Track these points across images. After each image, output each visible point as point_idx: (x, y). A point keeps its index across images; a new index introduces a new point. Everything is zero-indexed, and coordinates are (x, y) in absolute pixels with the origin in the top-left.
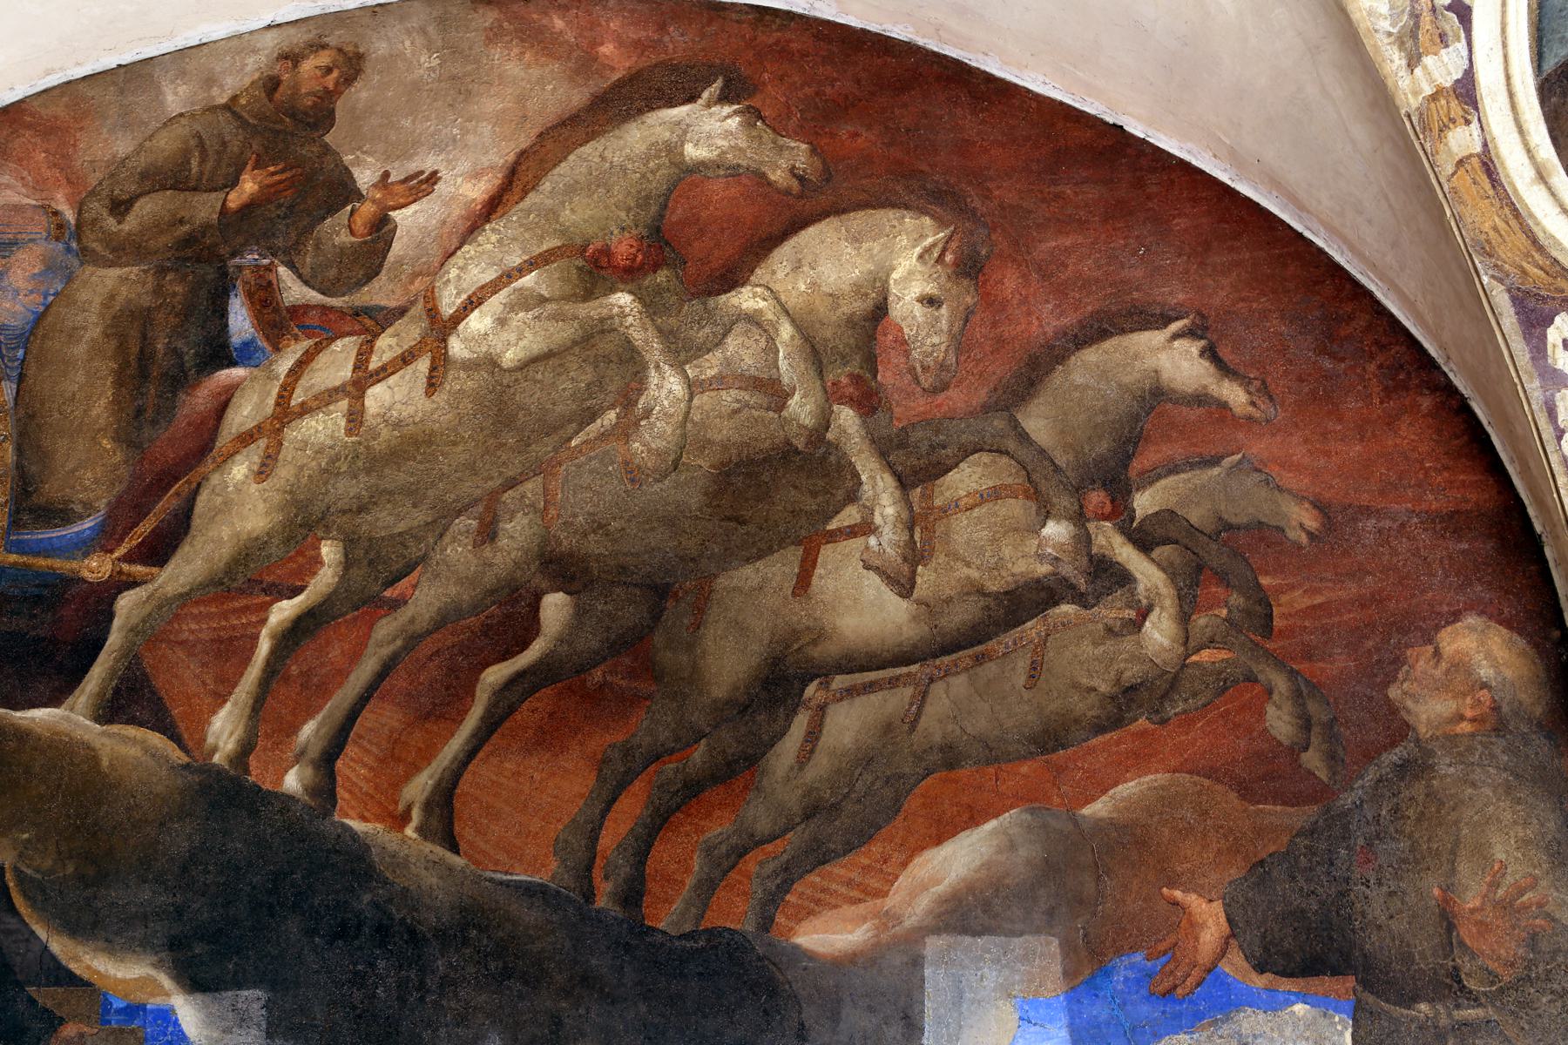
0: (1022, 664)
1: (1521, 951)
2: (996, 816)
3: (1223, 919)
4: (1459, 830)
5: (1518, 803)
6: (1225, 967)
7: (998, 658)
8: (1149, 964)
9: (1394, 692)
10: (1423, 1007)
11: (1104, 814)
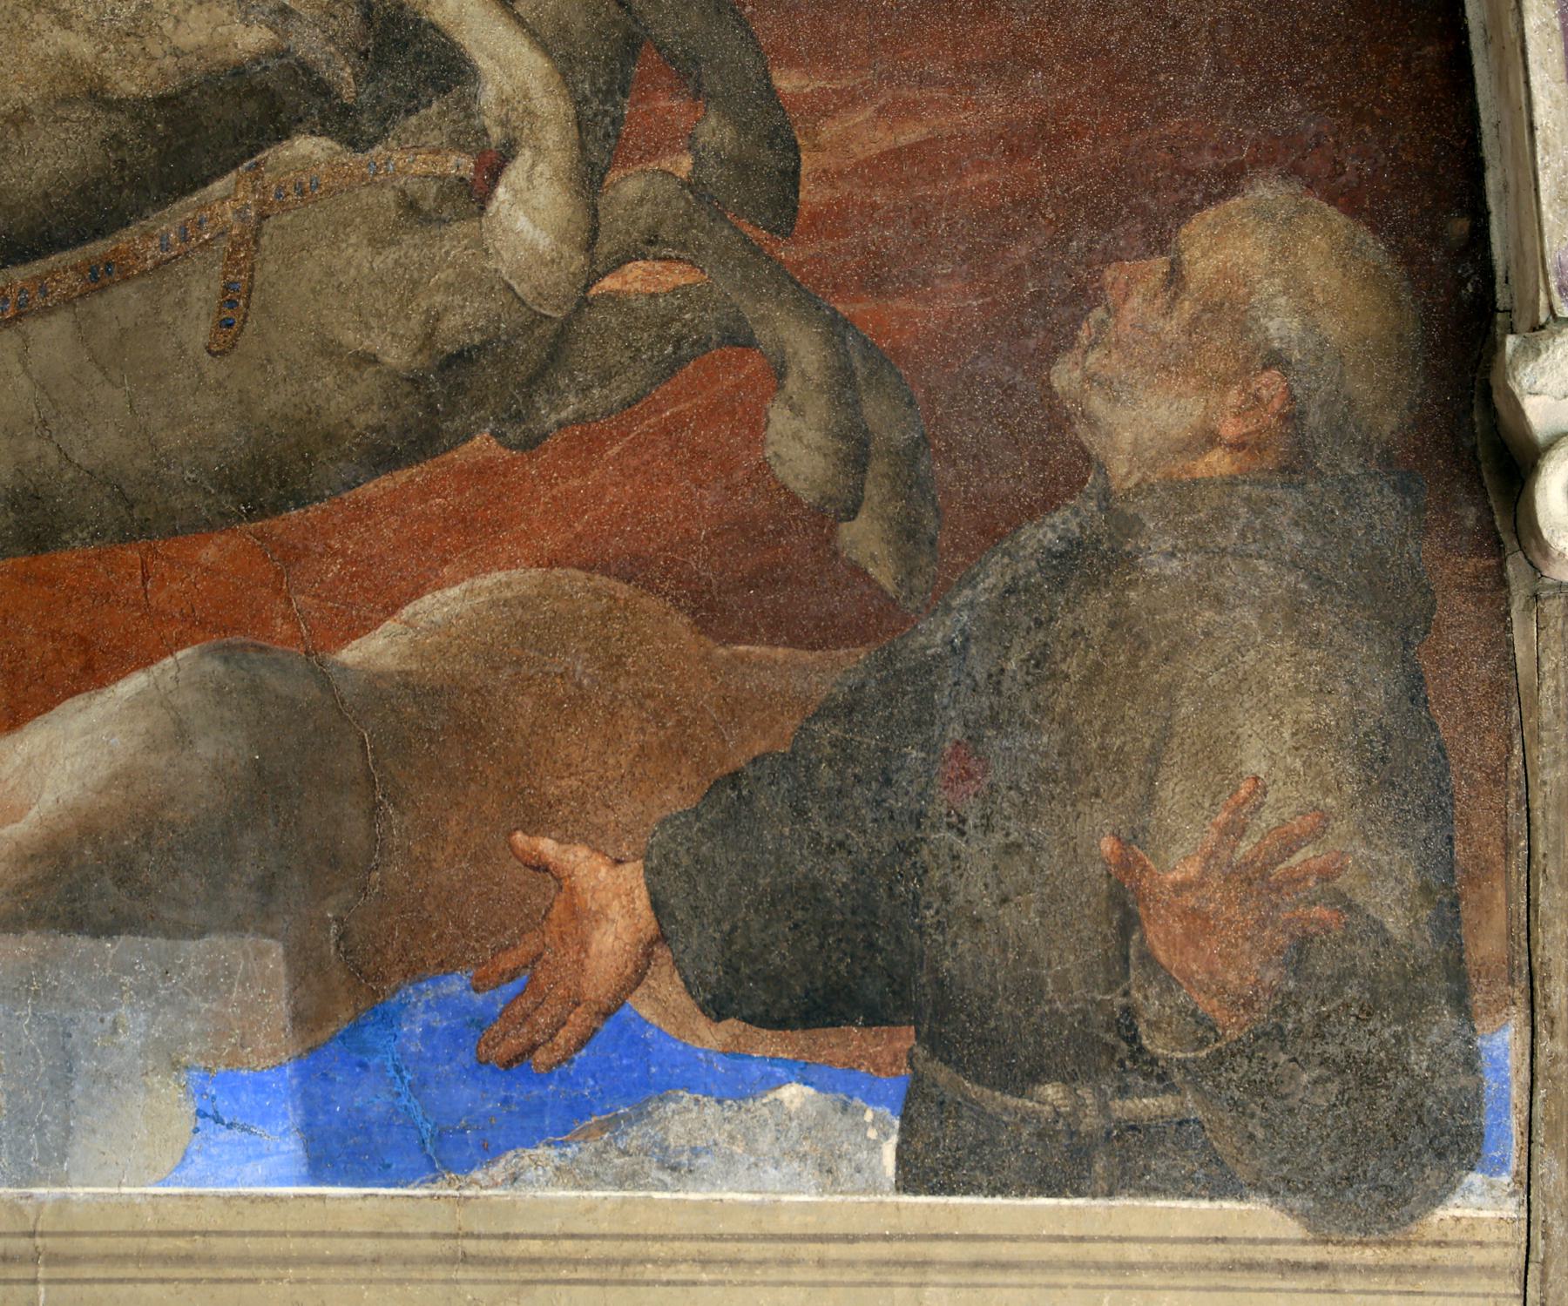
0: (203, 290)
1: (1271, 975)
2: (144, 662)
3: (642, 903)
4: (1173, 705)
5: (1312, 645)
6: (641, 1006)
7: (143, 273)
8: (479, 999)
9: (1064, 376)
10: (1051, 1091)
11: (389, 662)
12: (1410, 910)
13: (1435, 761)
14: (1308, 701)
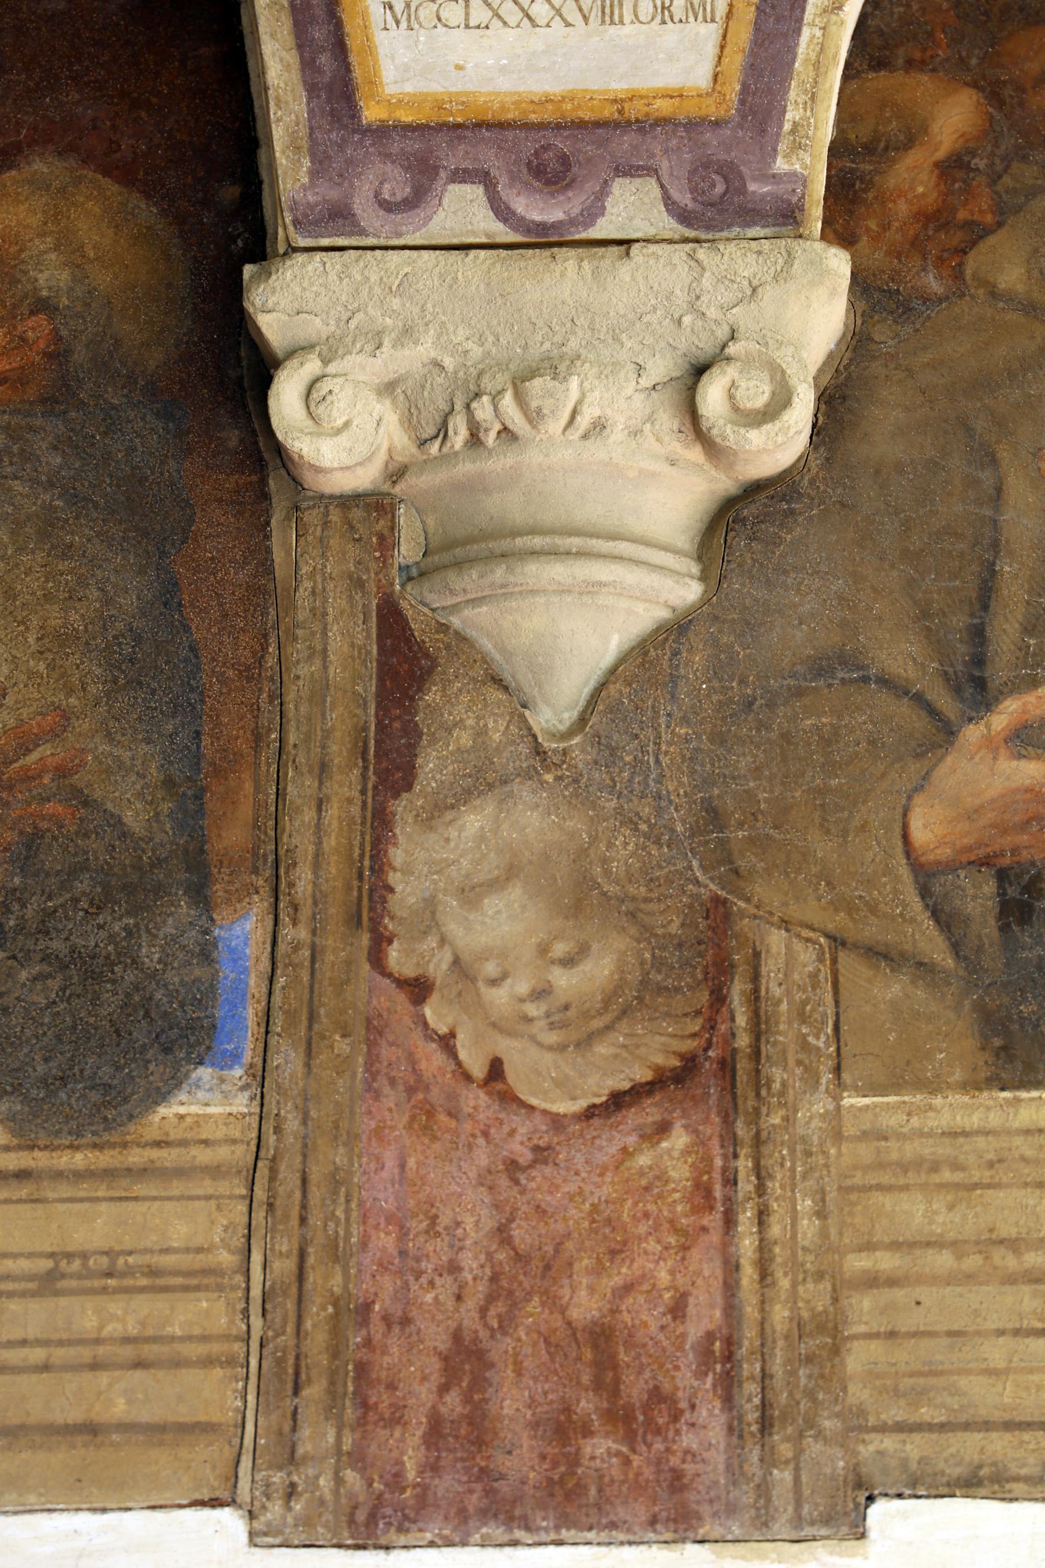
5: (64, 556)
12: (151, 803)
13: (186, 660)
14: (56, 607)
